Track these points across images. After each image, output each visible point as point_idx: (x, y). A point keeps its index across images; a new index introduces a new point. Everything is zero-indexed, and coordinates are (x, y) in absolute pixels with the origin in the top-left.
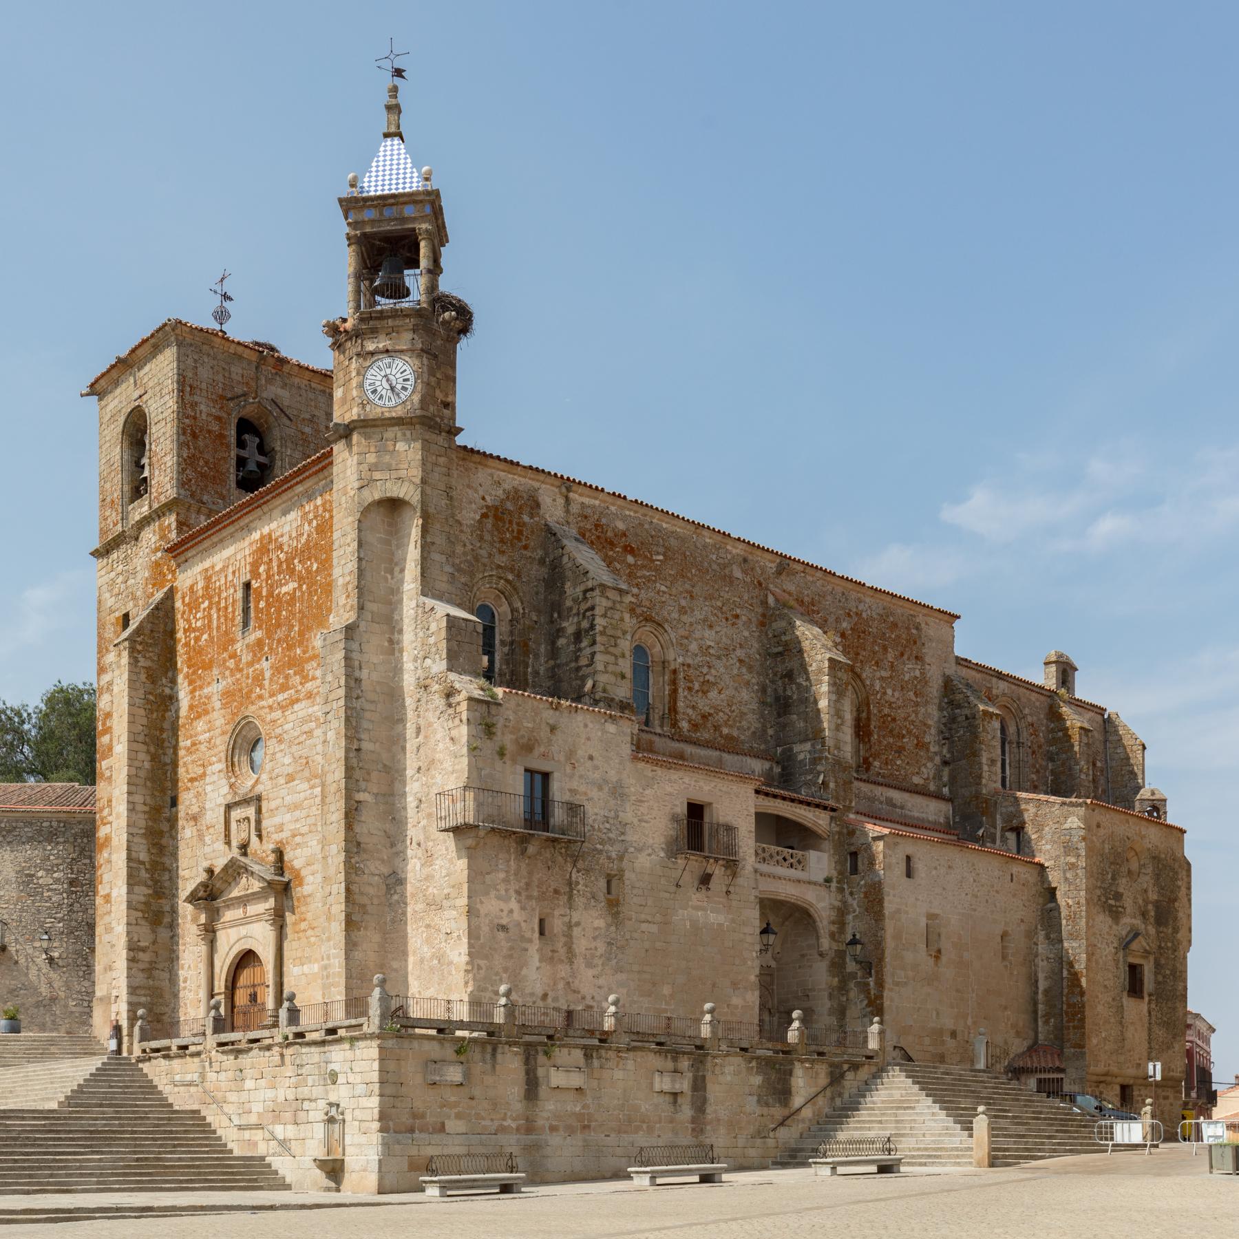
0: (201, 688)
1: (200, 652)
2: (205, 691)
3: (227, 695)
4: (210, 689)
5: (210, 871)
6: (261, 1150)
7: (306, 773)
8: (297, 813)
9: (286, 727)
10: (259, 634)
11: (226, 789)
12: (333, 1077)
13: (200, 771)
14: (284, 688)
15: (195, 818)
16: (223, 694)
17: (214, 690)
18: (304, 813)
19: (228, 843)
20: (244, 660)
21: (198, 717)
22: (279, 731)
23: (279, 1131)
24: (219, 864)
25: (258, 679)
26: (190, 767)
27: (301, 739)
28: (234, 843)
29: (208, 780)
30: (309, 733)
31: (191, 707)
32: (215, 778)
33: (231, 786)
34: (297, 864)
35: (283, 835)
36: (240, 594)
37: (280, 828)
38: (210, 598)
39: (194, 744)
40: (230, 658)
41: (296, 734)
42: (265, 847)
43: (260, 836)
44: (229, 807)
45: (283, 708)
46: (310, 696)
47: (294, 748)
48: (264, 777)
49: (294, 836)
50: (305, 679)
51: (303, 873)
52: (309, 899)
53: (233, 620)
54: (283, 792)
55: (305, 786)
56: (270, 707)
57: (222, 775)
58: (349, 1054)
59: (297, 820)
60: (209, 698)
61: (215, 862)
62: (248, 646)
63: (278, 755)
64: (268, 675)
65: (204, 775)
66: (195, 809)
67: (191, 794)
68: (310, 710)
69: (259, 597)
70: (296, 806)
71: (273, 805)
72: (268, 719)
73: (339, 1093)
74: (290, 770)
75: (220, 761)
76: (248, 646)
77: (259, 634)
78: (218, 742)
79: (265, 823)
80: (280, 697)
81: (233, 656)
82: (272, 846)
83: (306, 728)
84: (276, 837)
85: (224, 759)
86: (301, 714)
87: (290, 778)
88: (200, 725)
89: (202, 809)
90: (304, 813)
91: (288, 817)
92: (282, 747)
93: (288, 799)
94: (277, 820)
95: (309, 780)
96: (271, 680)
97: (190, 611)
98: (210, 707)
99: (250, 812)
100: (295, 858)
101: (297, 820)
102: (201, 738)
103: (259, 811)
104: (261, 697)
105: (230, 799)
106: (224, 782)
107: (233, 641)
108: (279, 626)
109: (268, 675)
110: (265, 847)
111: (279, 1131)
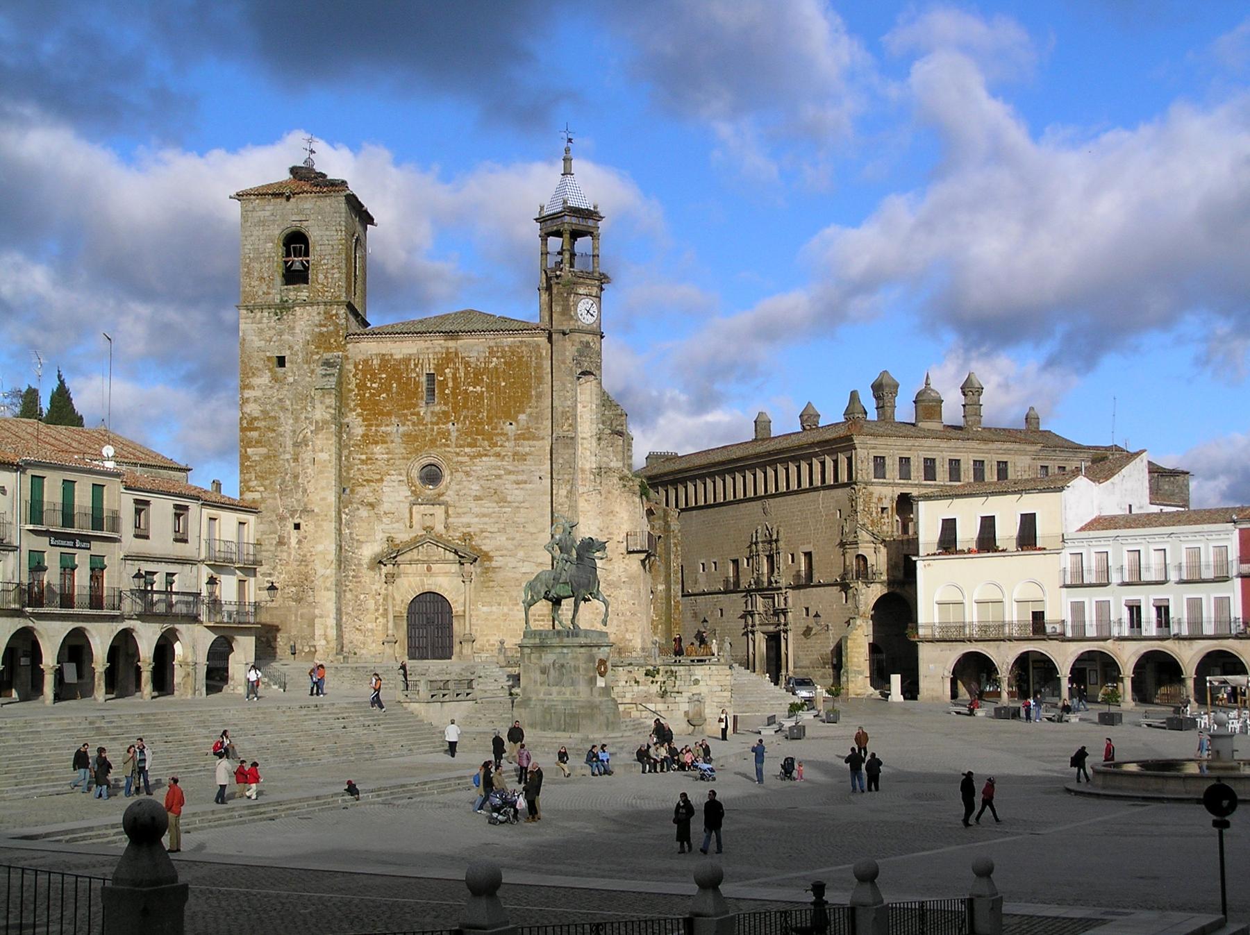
0: (377, 425)
1: (377, 403)
2: (383, 428)
3: (408, 438)
4: (389, 428)
6: (635, 714)
7: (495, 498)
10: (444, 408)
12: (696, 682)
14: (469, 445)
15: (372, 505)
16: (404, 435)
17: (394, 429)
18: (493, 520)
20: (428, 419)
21: (376, 443)
23: (651, 706)
24: (403, 536)
25: (446, 435)
26: (365, 473)
28: (416, 526)
30: (499, 477)
31: (365, 436)
34: (484, 548)
36: (424, 379)
38: (385, 371)
39: (368, 459)
40: (412, 414)
45: (472, 457)
46: (498, 455)
47: (482, 482)
48: (449, 492)
50: (495, 445)
53: (415, 393)
56: (458, 454)
58: (709, 672)
60: (388, 434)
62: (432, 413)
64: (454, 434)
65: (382, 480)
66: (372, 500)
67: (366, 489)
69: (444, 384)
70: (484, 515)
71: (460, 511)
72: (455, 459)
73: (702, 688)
76: (432, 413)
77: (444, 408)
79: (450, 520)
80: (467, 450)
81: (418, 414)
87: (477, 498)
88: (378, 449)
89: (379, 501)
90: (493, 520)
91: (476, 520)
93: (476, 510)
94: (465, 520)
96: (457, 439)
97: (364, 376)
98: (388, 439)
99: (439, 511)
102: (379, 457)
103: (447, 512)
104: (448, 446)
106: (406, 488)
107: (416, 405)
108: (464, 407)
109: (454, 434)
111: (651, 706)
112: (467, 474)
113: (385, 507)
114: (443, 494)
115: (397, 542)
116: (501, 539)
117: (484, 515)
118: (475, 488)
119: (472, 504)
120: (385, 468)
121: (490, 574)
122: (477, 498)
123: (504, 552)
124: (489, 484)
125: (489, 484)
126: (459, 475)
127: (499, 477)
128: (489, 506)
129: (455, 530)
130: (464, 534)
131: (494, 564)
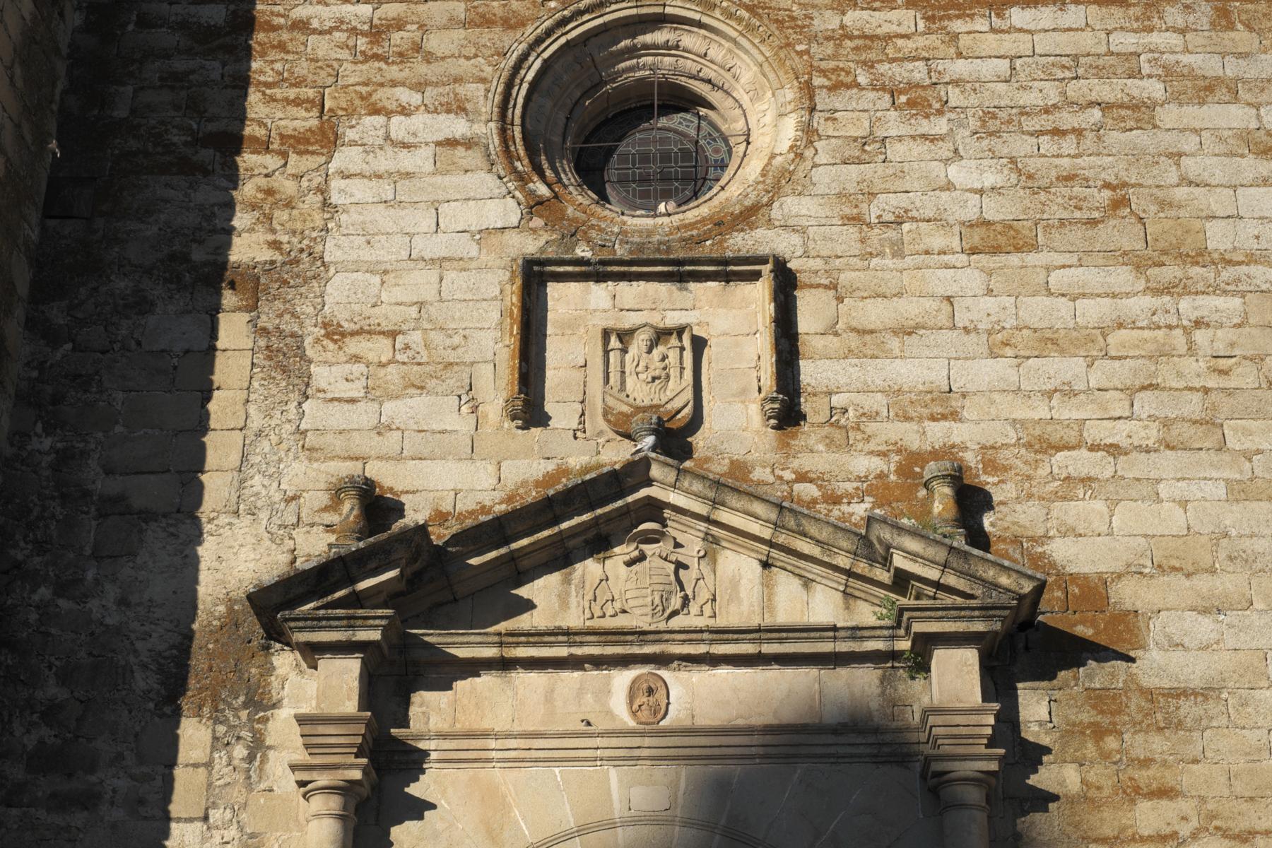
5: (377, 507)
8: (1068, 368)
9: (960, 68)
11: (506, 211)
13: (305, 120)
19: (530, 411)
22: (918, 72)
27: (1067, 119)
29: (344, 158)
30: (1140, 113)
32: (420, 160)
33: (535, 206)
34: (1073, 556)
35: (967, 435)
37: (943, 402)
41: (1030, 99)
42: (813, 451)
43: (788, 413)
44: (535, 278)
47: (1021, 146)
48: (790, 206)
49: (1048, 447)
51: (1126, 594)
52: (1188, 709)
54: (943, 282)
55: (1122, 277)
57: (473, 158)
59: (1069, 392)
61: (374, 471)
63: (896, 151)
65: (327, 138)
68: (1126, 41)
70: (1050, 342)
71: (874, 313)
74: (995, 210)
75: (459, 108)
78: (434, 43)
82: (864, 464)
83: (1107, 91)
84: (912, 436)
85: (487, 106)
86: (1065, 43)
87: (992, 240)
90: (1121, 372)
92: (940, 125)
94: (914, 370)
95: (1140, 266)
100: (1076, 534)
101: (1069, 392)
105: (531, 245)
106: (485, 182)
110: (805, 462)
112: (916, 100)
113: (341, 295)
114: (748, 216)
115: (415, 514)
116: (1185, 498)
117: (1050, 342)
118: (974, 179)
119: (966, 278)
120: (353, 74)
121: (1138, 744)
122: (992, 240)
123: (1229, 583)
124: (1054, 156)
125: (1054, 156)
126: (854, 113)
127: (1140, 113)
128: (1087, 288)
129: (843, 430)
130: (911, 462)
131: (1156, 665)
